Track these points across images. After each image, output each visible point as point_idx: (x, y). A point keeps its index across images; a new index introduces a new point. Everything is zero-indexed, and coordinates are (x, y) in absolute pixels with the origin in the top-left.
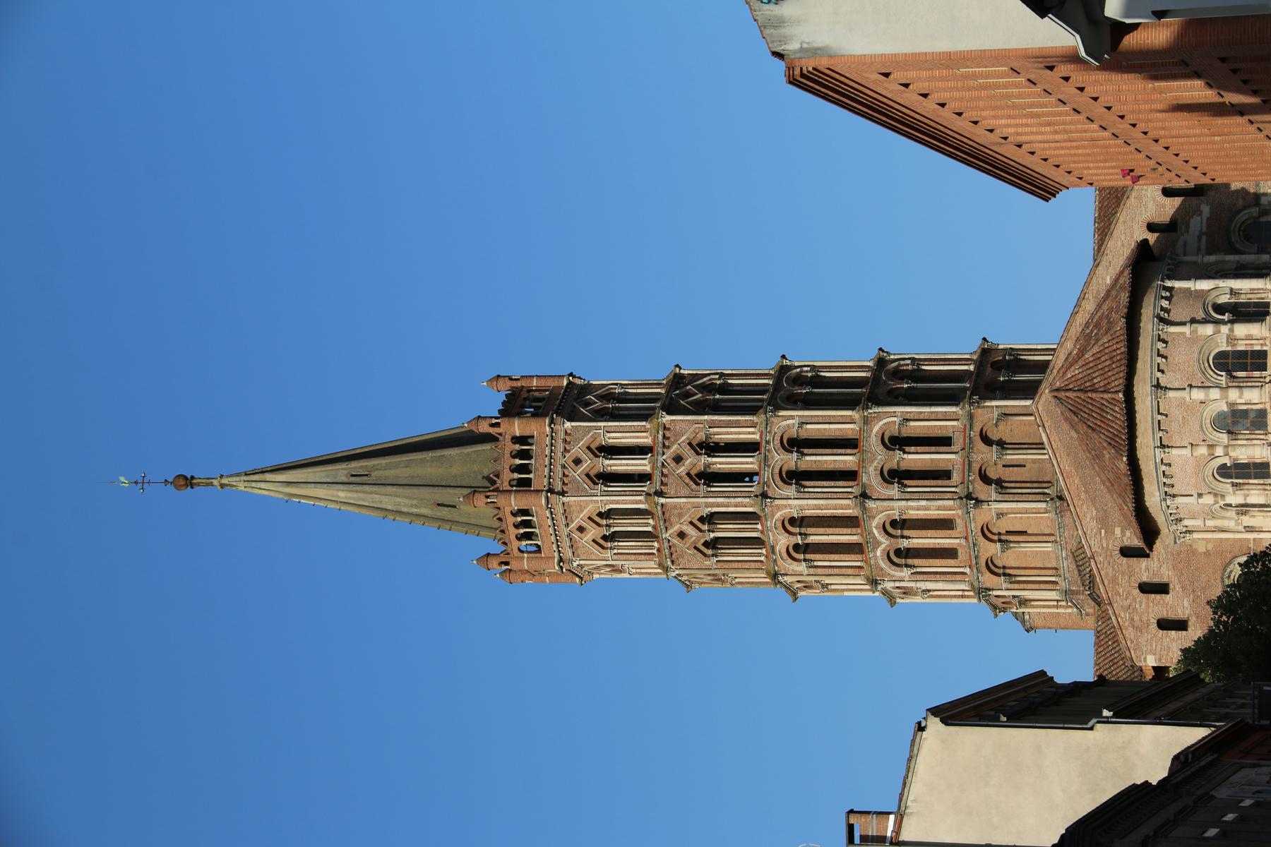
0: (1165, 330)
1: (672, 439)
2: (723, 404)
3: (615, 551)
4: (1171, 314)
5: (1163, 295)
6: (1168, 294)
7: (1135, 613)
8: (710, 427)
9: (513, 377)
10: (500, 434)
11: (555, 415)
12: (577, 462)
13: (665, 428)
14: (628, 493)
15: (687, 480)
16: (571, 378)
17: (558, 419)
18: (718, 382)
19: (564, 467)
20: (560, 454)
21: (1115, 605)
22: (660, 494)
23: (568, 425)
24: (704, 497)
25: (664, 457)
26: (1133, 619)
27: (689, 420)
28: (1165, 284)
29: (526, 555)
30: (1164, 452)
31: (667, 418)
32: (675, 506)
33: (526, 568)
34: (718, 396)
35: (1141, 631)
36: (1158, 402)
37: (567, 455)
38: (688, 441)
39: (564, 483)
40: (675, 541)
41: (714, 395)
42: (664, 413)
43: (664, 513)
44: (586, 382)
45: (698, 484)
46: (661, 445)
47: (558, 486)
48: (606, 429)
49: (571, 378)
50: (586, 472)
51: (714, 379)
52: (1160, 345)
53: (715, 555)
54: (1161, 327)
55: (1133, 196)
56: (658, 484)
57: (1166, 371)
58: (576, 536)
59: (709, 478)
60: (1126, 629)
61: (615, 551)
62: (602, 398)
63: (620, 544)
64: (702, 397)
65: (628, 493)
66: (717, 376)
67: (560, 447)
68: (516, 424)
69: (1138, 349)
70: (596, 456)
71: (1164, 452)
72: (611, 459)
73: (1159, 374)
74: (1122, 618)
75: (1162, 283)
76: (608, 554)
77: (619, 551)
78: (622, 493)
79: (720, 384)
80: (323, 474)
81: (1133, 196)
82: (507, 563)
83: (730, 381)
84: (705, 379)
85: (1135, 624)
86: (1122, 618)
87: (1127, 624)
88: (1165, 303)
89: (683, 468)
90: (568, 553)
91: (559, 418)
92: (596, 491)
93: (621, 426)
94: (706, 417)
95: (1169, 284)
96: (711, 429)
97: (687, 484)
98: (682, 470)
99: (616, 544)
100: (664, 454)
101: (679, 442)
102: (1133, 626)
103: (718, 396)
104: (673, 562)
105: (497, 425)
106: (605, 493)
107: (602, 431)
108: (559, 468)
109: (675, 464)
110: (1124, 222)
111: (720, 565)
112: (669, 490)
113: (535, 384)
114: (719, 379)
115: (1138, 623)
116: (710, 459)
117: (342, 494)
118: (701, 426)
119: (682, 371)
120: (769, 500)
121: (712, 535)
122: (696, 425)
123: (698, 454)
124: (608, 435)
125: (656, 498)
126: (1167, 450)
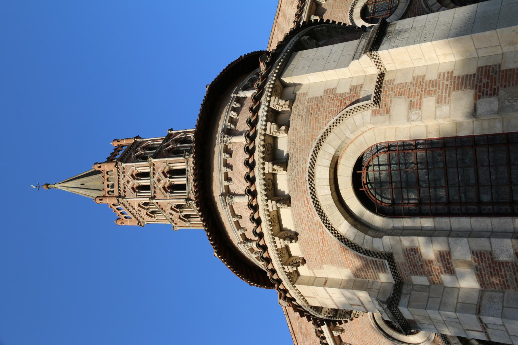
0: (229, 141)
1: (156, 171)
2: (181, 149)
3: (156, 218)
4: (238, 124)
5: (234, 106)
6: (238, 105)
7: (302, 323)
8: (169, 164)
9: (119, 140)
10: (103, 171)
11: (118, 161)
12: (128, 182)
13: (154, 165)
14: (146, 196)
15: (163, 191)
16: (135, 139)
17: (119, 163)
18: (183, 137)
19: (123, 185)
20: (121, 179)
21: (290, 316)
22: (154, 198)
23: (124, 165)
24: (169, 199)
25: (154, 180)
26: (301, 327)
27: (161, 161)
28: (238, 95)
29: (128, 220)
30: (247, 246)
31: (154, 161)
32: (161, 202)
33: (129, 225)
34: (179, 145)
35: (306, 337)
36: (231, 207)
37: (125, 179)
38: (162, 171)
39: (125, 192)
40: (171, 216)
41: (177, 145)
42: (152, 158)
43: (160, 206)
44: (142, 140)
45: (167, 192)
46: (152, 174)
47: (123, 194)
48: (136, 166)
49: (135, 139)
50: (131, 187)
51: (181, 135)
52: (225, 156)
53: (189, 221)
54: (225, 139)
55: (281, 16)
56: (153, 193)
57: (233, 179)
58: (139, 212)
59: (173, 188)
60: (298, 335)
61: (156, 218)
62: (144, 148)
63: (158, 215)
64: (173, 146)
65: (146, 196)
66: (182, 134)
67: (121, 175)
68: (106, 166)
69: (214, 159)
70: (134, 178)
71: (247, 246)
72: (141, 180)
73: (226, 183)
74: (295, 326)
75: (235, 95)
76: (153, 219)
77: (158, 218)
78: (144, 196)
79: (184, 137)
80: (75, 184)
81: (281, 16)
82: (123, 223)
83: (188, 135)
84: (178, 136)
85: (303, 330)
86: (295, 326)
87: (298, 330)
88: (233, 114)
89: (161, 185)
90: (141, 219)
91: (120, 162)
92: (134, 196)
93: (141, 164)
94: (166, 159)
95: (241, 94)
96: (170, 165)
97: (163, 193)
98: (161, 186)
99: (156, 215)
100: (154, 177)
101: (158, 172)
102: (301, 332)
103: (179, 145)
104: (176, 224)
105: (100, 167)
106: (138, 197)
107: (134, 167)
108: (122, 185)
109: (158, 183)
110: (277, 35)
111: (193, 225)
112: (158, 197)
113: (125, 143)
114: (183, 135)
115: (304, 331)
116: (170, 180)
117: (81, 191)
118: (165, 163)
119: (172, 132)
120: (190, 201)
121: (183, 214)
122: (164, 163)
123: (166, 177)
124: (137, 169)
125: (151, 200)
126: (249, 244)
